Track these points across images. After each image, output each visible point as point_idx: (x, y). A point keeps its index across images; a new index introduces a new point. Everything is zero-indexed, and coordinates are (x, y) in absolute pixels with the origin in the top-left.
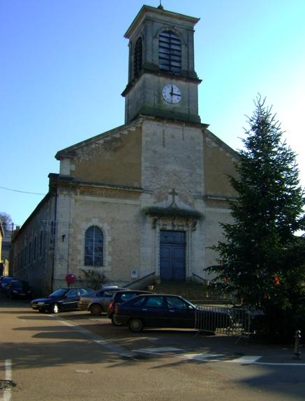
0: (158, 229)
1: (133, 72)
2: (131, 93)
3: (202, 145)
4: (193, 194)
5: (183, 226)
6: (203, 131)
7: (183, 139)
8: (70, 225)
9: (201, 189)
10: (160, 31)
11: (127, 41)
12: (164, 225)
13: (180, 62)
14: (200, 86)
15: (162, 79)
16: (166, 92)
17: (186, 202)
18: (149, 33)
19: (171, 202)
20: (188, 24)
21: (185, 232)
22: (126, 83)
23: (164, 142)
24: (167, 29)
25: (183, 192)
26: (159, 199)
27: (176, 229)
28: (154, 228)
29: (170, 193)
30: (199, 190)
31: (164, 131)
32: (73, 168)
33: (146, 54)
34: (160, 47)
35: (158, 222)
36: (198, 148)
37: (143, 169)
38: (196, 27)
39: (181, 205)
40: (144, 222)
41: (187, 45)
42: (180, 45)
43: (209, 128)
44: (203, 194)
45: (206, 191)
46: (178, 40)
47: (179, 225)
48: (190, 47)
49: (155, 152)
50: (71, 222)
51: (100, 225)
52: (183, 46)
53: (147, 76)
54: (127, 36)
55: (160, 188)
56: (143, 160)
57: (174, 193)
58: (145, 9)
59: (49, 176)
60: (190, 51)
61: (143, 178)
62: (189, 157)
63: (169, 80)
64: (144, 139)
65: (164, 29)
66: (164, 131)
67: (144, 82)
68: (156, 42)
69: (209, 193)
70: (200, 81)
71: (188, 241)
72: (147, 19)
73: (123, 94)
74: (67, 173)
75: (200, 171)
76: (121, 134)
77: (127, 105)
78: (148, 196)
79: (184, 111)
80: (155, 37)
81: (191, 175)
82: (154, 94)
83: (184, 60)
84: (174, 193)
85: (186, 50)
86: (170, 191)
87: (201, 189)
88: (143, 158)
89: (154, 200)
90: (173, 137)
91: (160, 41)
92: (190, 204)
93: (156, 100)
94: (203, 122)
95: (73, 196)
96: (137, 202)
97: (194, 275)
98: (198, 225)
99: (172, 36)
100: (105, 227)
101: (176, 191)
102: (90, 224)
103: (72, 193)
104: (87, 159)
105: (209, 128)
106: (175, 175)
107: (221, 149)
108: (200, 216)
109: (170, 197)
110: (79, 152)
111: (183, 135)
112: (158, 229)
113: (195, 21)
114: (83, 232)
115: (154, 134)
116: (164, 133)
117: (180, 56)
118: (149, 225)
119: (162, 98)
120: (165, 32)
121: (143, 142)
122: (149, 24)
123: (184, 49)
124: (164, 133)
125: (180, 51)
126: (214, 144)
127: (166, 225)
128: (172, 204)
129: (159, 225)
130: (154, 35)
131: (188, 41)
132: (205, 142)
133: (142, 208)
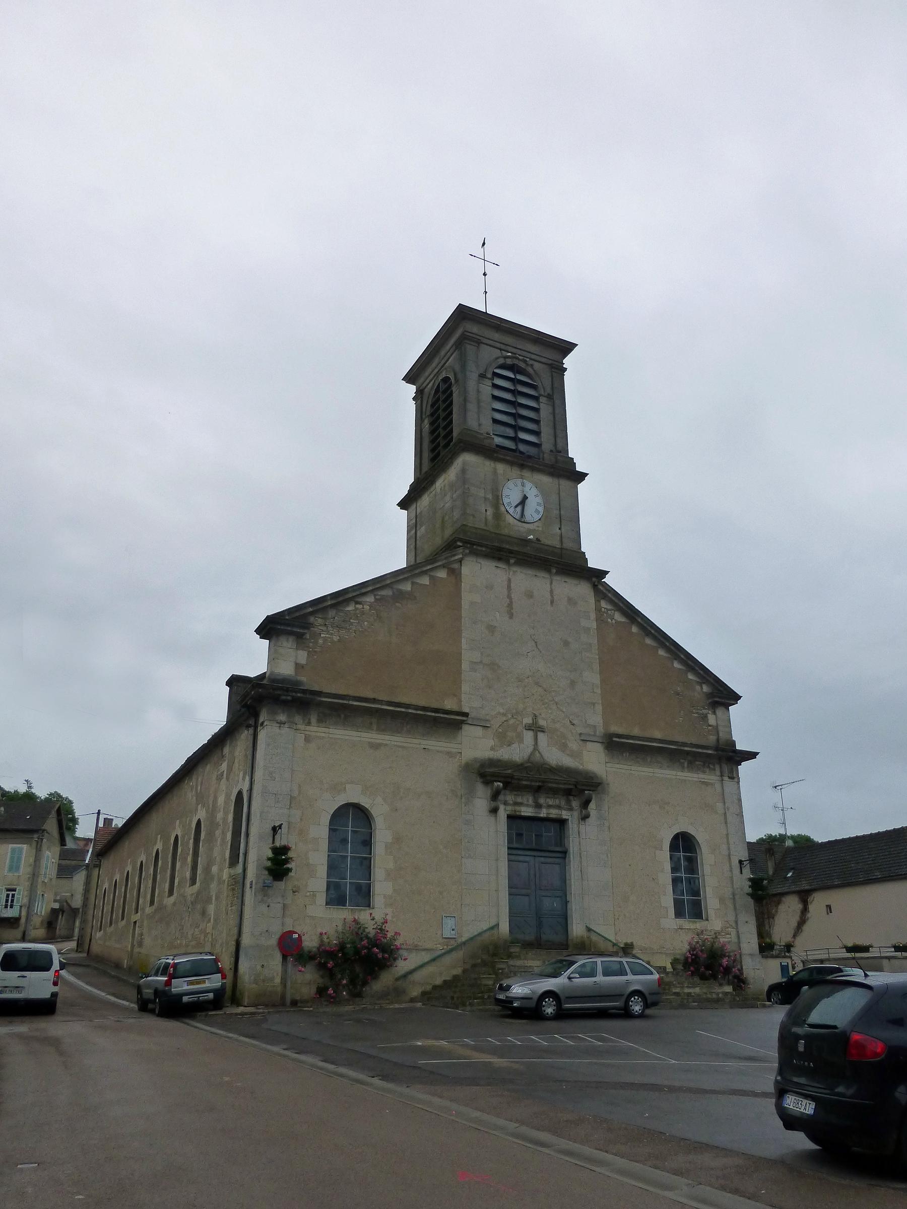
0: (502, 813)
1: (426, 455)
2: (425, 501)
3: (593, 616)
4: (579, 730)
5: (559, 807)
6: (595, 587)
7: (552, 602)
8: (292, 798)
9: (596, 719)
10: (495, 365)
11: (412, 389)
12: (516, 804)
13: (537, 433)
14: (583, 488)
15: (501, 468)
16: (511, 494)
17: (563, 747)
18: (471, 366)
19: (531, 749)
20: (550, 354)
21: (562, 823)
22: (409, 478)
23: (510, 605)
24: (509, 361)
25: (558, 726)
26: (503, 738)
27: (543, 813)
28: (494, 811)
29: (529, 728)
30: (590, 722)
31: (509, 581)
32: (302, 657)
33: (464, 410)
34: (495, 398)
35: (501, 797)
36: (584, 623)
37: (465, 666)
38: (568, 362)
39: (553, 756)
40: (471, 793)
41: (550, 397)
42: (536, 398)
43: (607, 580)
44: (600, 730)
45: (606, 724)
46: (534, 387)
47: (550, 808)
48: (557, 402)
49: (491, 629)
50: (295, 794)
51: (365, 802)
52: (542, 399)
53: (467, 458)
54: (410, 378)
55: (504, 715)
56: (464, 646)
57: (535, 728)
58: (463, 314)
59: (229, 683)
60: (557, 411)
61: (465, 688)
62: (566, 643)
63: (516, 471)
64: (467, 598)
65: (501, 361)
66: (509, 581)
67: (463, 471)
68: (486, 389)
69: (615, 729)
70: (582, 476)
71: (573, 845)
72: (464, 338)
73: (404, 504)
74: (286, 669)
75: (593, 677)
76: (413, 583)
77: (413, 527)
78: (479, 731)
79: (551, 540)
80: (482, 376)
81: (573, 684)
82: (486, 499)
83: (546, 430)
84: (535, 728)
85: (550, 409)
86: (528, 720)
87: (596, 719)
88: (463, 641)
89: (492, 743)
90: (530, 595)
91: (495, 386)
92: (574, 755)
93: (490, 512)
94: (593, 563)
95: (301, 727)
96: (452, 747)
97: (589, 930)
98: (592, 805)
99: (519, 377)
100: (378, 809)
101: (542, 722)
102: (342, 800)
103: (298, 719)
104: (336, 638)
105: (607, 580)
106: (537, 684)
107: (634, 629)
108: (600, 784)
109: (528, 736)
110: (317, 621)
111: (551, 592)
112: (502, 813)
113: (566, 347)
114: (326, 819)
115: (490, 587)
116: (509, 587)
117: (537, 422)
118: (481, 802)
119: (503, 509)
120: (502, 367)
121: (465, 604)
122: (470, 348)
123: (545, 411)
124: (509, 587)
125: (536, 410)
126: (618, 617)
127: (521, 804)
128: (532, 754)
129: (505, 803)
130: (482, 371)
131: (552, 388)
132: (598, 609)
133: (463, 762)
